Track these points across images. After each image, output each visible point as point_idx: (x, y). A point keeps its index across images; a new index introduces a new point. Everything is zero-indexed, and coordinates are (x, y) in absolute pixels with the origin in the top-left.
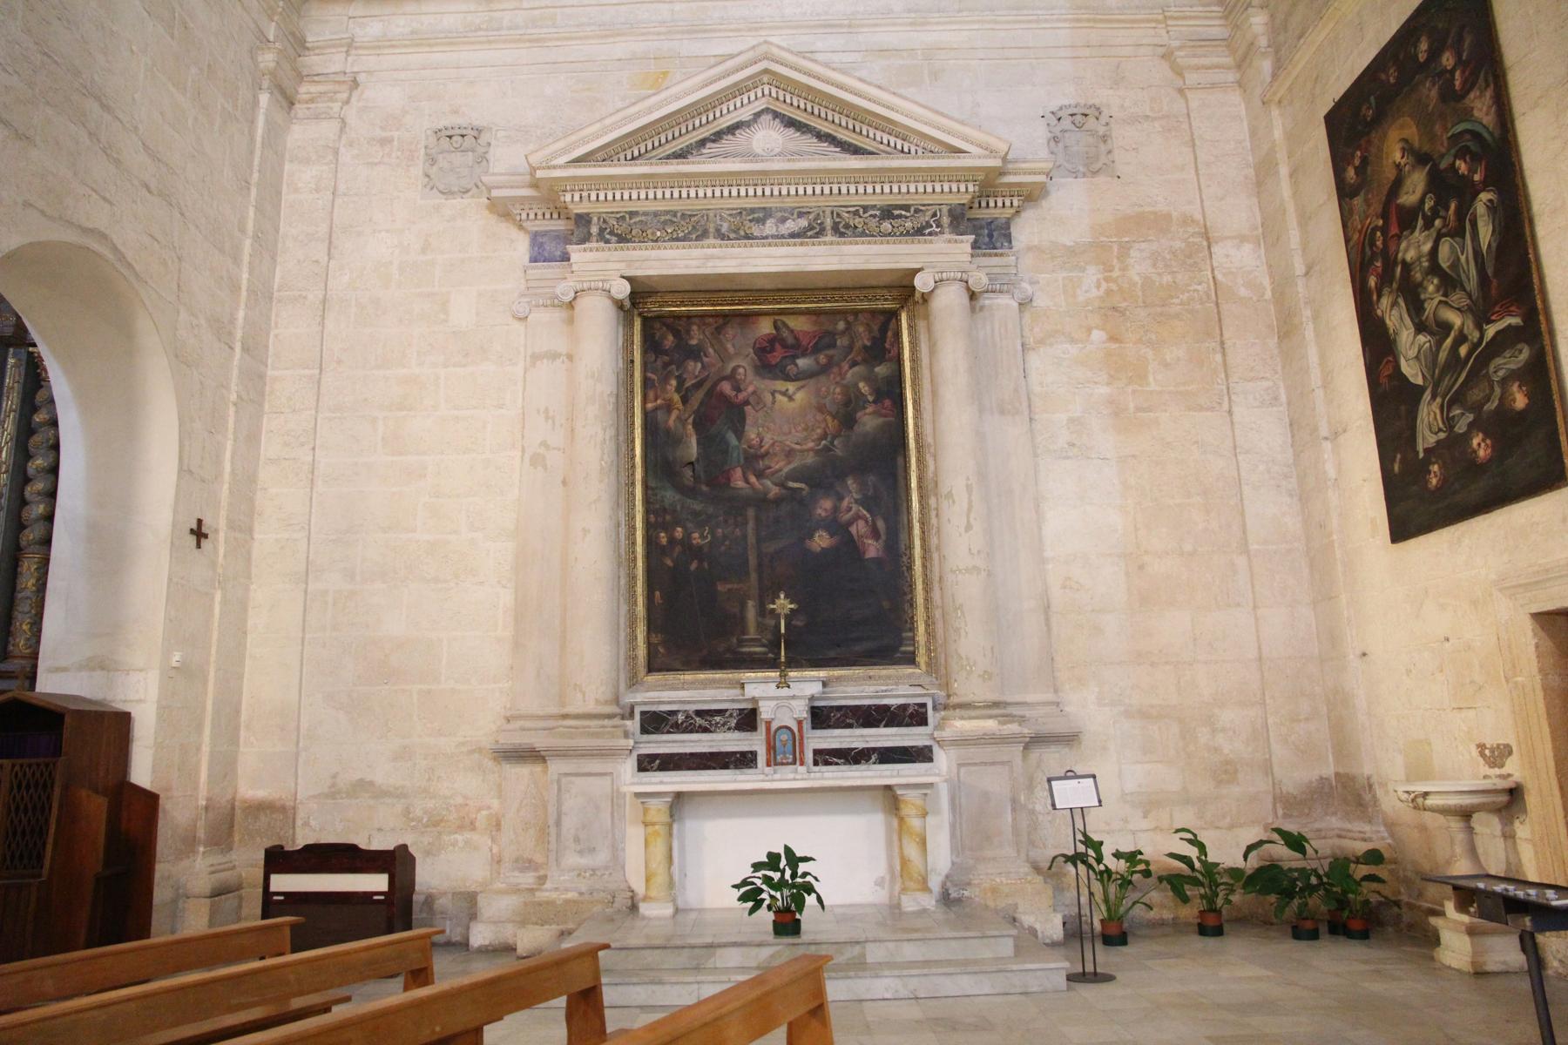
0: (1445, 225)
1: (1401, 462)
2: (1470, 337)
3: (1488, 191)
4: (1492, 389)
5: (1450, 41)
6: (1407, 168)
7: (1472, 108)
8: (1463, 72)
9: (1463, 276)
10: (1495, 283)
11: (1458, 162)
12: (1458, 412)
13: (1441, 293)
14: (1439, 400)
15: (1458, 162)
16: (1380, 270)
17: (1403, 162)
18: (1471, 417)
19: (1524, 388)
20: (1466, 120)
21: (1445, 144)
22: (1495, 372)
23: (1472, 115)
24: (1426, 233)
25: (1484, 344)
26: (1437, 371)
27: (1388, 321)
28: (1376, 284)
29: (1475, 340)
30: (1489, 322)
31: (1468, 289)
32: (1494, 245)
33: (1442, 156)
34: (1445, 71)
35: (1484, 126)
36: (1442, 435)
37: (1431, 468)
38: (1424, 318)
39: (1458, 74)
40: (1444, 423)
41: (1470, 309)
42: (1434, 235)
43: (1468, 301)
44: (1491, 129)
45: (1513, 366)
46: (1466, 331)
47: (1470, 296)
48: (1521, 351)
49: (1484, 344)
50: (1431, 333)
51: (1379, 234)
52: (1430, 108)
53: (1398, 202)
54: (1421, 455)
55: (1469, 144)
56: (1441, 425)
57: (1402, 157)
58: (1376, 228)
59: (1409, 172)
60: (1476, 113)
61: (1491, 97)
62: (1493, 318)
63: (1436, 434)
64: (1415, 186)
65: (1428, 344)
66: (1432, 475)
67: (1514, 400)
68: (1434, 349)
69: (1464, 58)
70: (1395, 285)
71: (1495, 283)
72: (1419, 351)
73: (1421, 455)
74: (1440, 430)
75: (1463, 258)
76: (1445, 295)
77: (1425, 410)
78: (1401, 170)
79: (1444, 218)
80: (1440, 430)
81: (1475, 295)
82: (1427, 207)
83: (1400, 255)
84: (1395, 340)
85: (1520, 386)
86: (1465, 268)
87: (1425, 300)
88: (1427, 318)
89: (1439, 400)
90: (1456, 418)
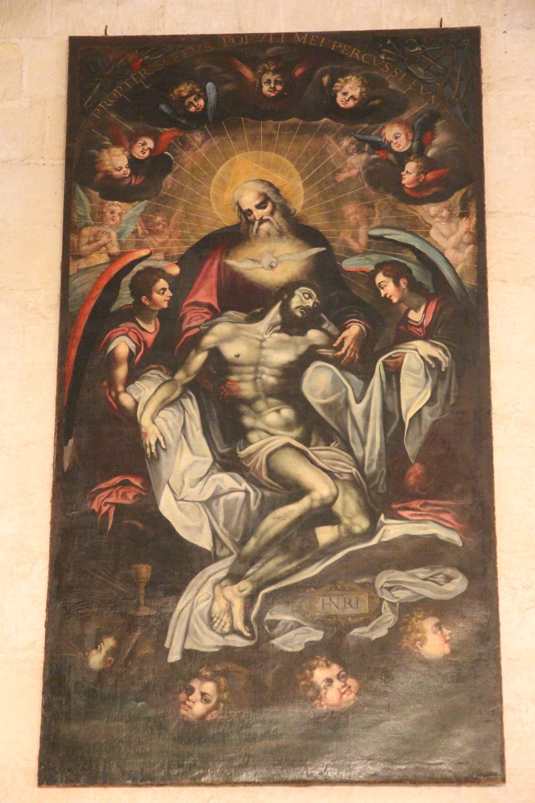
0: (329, 346)
1: (114, 652)
2: (346, 521)
3: (433, 344)
4: (378, 612)
5: (406, 116)
6: (265, 226)
7: (431, 226)
8: (423, 170)
9: (351, 432)
10: (417, 469)
11: (380, 278)
12: (289, 618)
13: (296, 433)
14: (246, 586)
15: (380, 278)
16: (150, 338)
17: (258, 213)
18: (317, 636)
19: (446, 631)
20: (411, 233)
21: (363, 240)
22: (389, 589)
23: (427, 234)
24: (284, 336)
25: (375, 541)
26: (252, 542)
27: (145, 421)
28: (131, 356)
29: (357, 530)
30: (394, 515)
31: (359, 454)
32: (428, 419)
33: (351, 253)
34: (385, 147)
35: (447, 261)
36: (238, 642)
37: (195, 684)
38: (242, 453)
39: (411, 166)
40: (247, 622)
41: (355, 483)
42: (303, 349)
43: (354, 470)
44: (458, 270)
45: (428, 593)
46: (338, 508)
47: (359, 465)
48: (449, 579)
49: (375, 541)
50: (254, 481)
51: (162, 283)
52: (341, 177)
53: (231, 262)
54: (174, 656)
55: (409, 265)
56: (239, 624)
57: (258, 207)
58: (161, 273)
59: (268, 234)
60: (433, 233)
61: (467, 232)
62: (405, 514)
63: (223, 635)
64: (278, 262)
65: (242, 495)
66: (196, 696)
67: (423, 640)
68: (254, 507)
69: (429, 154)
70: (180, 376)
71: (417, 469)
72: (215, 496)
73: (174, 656)
74: (234, 631)
75: (357, 409)
76: (306, 440)
77: (207, 589)
78: (252, 223)
79: (332, 338)
80: (234, 631)
81: (371, 467)
82: (295, 302)
83: (209, 340)
84: (156, 459)
85: (439, 626)
86: (360, 423)
87: (253, 429)
88: (250, 456)
89: (246, 586)
90: (280, 628)
